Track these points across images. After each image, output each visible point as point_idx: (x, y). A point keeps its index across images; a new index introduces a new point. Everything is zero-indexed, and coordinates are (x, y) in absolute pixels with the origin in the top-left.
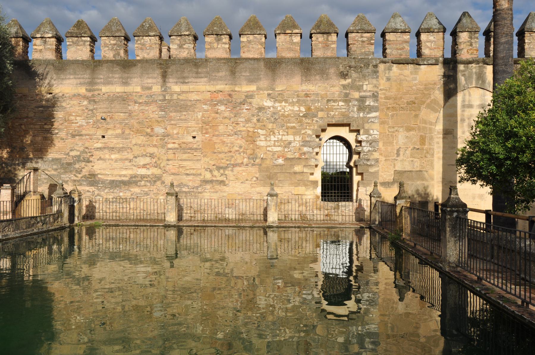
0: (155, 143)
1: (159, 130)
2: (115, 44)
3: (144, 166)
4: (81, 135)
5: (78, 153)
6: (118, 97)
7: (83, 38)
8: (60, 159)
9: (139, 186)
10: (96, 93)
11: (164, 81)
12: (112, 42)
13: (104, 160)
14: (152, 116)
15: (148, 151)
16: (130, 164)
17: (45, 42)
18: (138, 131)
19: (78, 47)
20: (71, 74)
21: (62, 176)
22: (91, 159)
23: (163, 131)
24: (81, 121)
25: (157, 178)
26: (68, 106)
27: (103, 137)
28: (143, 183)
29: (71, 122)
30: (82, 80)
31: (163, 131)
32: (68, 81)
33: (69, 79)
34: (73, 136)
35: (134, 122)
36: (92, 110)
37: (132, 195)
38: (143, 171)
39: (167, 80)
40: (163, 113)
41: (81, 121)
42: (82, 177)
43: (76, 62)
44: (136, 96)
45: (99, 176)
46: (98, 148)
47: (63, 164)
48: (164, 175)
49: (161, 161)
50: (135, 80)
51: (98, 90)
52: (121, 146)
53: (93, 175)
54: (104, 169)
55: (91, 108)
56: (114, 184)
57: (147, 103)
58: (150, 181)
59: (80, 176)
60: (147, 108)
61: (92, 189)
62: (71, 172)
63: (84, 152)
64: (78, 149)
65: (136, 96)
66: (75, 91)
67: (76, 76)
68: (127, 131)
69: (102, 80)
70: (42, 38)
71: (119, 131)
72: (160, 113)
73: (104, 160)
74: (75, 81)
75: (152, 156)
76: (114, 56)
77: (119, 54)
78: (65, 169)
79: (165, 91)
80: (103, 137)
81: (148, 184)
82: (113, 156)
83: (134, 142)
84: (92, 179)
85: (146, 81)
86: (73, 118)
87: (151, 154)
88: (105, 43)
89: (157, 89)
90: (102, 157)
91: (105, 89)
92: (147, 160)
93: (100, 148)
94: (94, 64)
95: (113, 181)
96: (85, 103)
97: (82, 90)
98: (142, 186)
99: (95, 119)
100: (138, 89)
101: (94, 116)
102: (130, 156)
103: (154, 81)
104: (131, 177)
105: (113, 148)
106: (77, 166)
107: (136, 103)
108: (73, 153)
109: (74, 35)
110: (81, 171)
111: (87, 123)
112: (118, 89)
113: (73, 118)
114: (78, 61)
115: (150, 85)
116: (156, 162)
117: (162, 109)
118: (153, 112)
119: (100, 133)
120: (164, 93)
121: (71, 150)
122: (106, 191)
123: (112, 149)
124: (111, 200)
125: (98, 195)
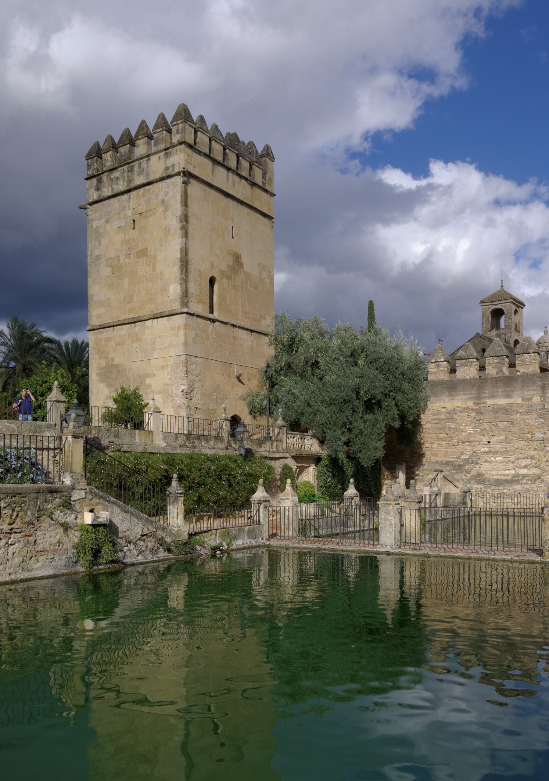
0: (535, 446)
1: (539, 435)
2: (497, 363)
3: (525, 467)
4: (470, 442)
5: (468, 457)
6: (501, 408)
7: (470, 360)
8: (453, 462)
9: (521, 484)
10: (482, 405)
11: (544, 392)
12: (495, 361)
13: (490, 462)
14: (532, 423)
15: (528, 453)
16: (512, 465)
17: (438, 366)
18: (519, 437)
19: (466, 368)
20: (461, 391)
21: (455, 476)
22: (479, 461)
23: (543, 436)
24: (470, 430)
25: (539, 477)
26: (459, 418)
27: (489, 442)
28: (524, 481)
29: (461, 431)
30: (469, 395)
31: (543, 436)
32: (459, 397)
33: (459, 395)
34: (463, 443)
35: (516, 429)
36: (478, 420)
37: (514, 491)
38: (524, 471)
39: (546, 391)
40: (542, 420)
41: (470, 430)
42: (471, 477)
43: (465, 381)
44: (517, 407)
45: (486, 476)
46: (484, 452)
47: (455, 466)
48: (544, 474)
49: (540, 462)
50: (517, 393)
51: (484, 403)
52: (505, 449)
53: (479, 475)
54: (490, 470)
55: (478, 418)
56: (499, 483)
57: (527, 413)
58: (531, 480)
59: (469, 475)
60: (528, 417)
61: (480, 486)
62: (462, 472)
63: (472, 455)
64: (467, 453)
65: (517, 407)
66: (464, 405)
67: (465, 393)
68: (510, 437)
69: (487, 395)
70: (435, 362)
71: (502, 437)
72: (540, 420)
73: (490, 462)
74: (464, 397)
75: (532, 458)
76: (497, 373)
77: (501, 371)
78: (457, 470)
79: (544, 400)
80: (489, 442)
81: (530, 482)
82: (498, 459)
83: (516, 446)
84: (480, 478)
85: (526, 393)
86: (463, 427)
87: (532, 456)
88: (489, 363)
89: (536, 399)
90: (488, 459)
91: (490, 402)
92: (529, 462)
93: (486, 452)
94: (480, 384)
95: (498, 480)
96: (473, 414)
97: (471, 404)
98: (524, 484)
99: (482, 427)
100: (520, 400)
101: (480, 426)
102: (513, 458)
103: (534, 392)
104: (514, 477)
105: (498, 452)
106: (467, 467)
107: (517, 412)
108: (463, 457)
109: (463, 358)
110: (470, 471)
111: (475, 431)
112: (502, 401)
113: (463, 427)
114: (467, 379)
115: (530, 396)
116: (536, 463)
117: (541, 416)
118: (532, 420)
119: (485, 439)
120: (543, 403)
121: (462, 455)
122: (492, 487)
123: (497, 453)
124: (496, 495)
125: (485, 491)
